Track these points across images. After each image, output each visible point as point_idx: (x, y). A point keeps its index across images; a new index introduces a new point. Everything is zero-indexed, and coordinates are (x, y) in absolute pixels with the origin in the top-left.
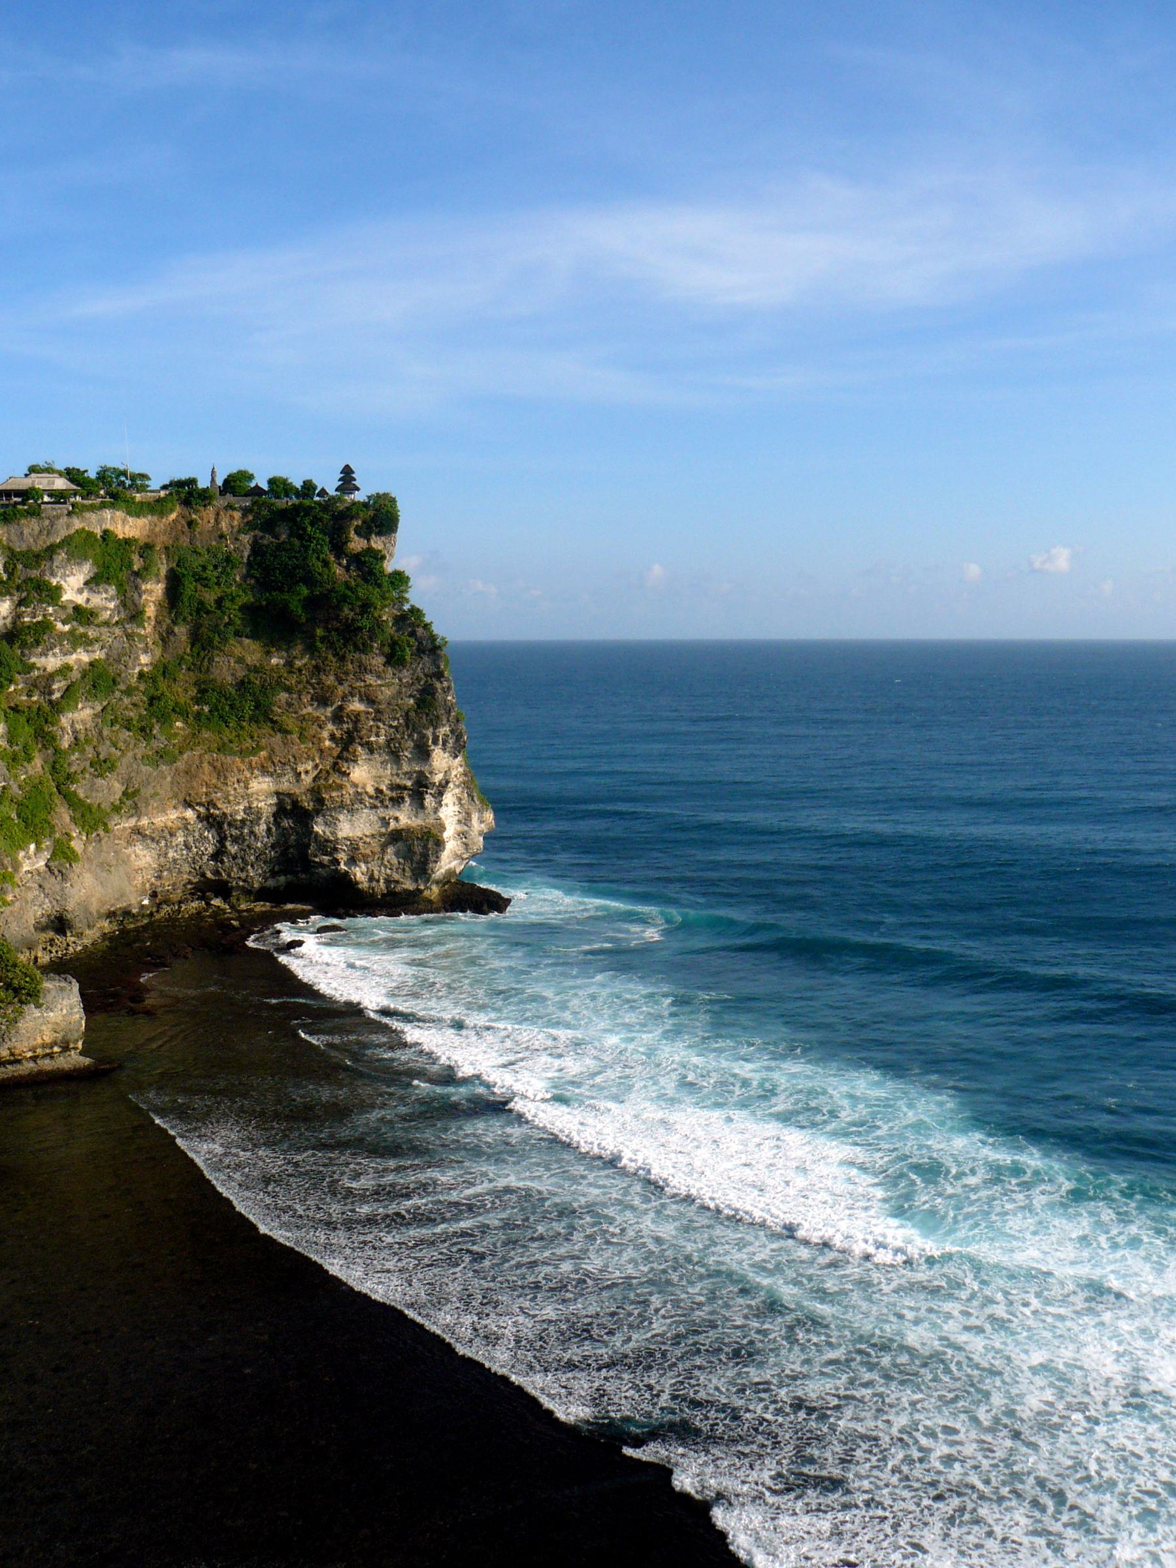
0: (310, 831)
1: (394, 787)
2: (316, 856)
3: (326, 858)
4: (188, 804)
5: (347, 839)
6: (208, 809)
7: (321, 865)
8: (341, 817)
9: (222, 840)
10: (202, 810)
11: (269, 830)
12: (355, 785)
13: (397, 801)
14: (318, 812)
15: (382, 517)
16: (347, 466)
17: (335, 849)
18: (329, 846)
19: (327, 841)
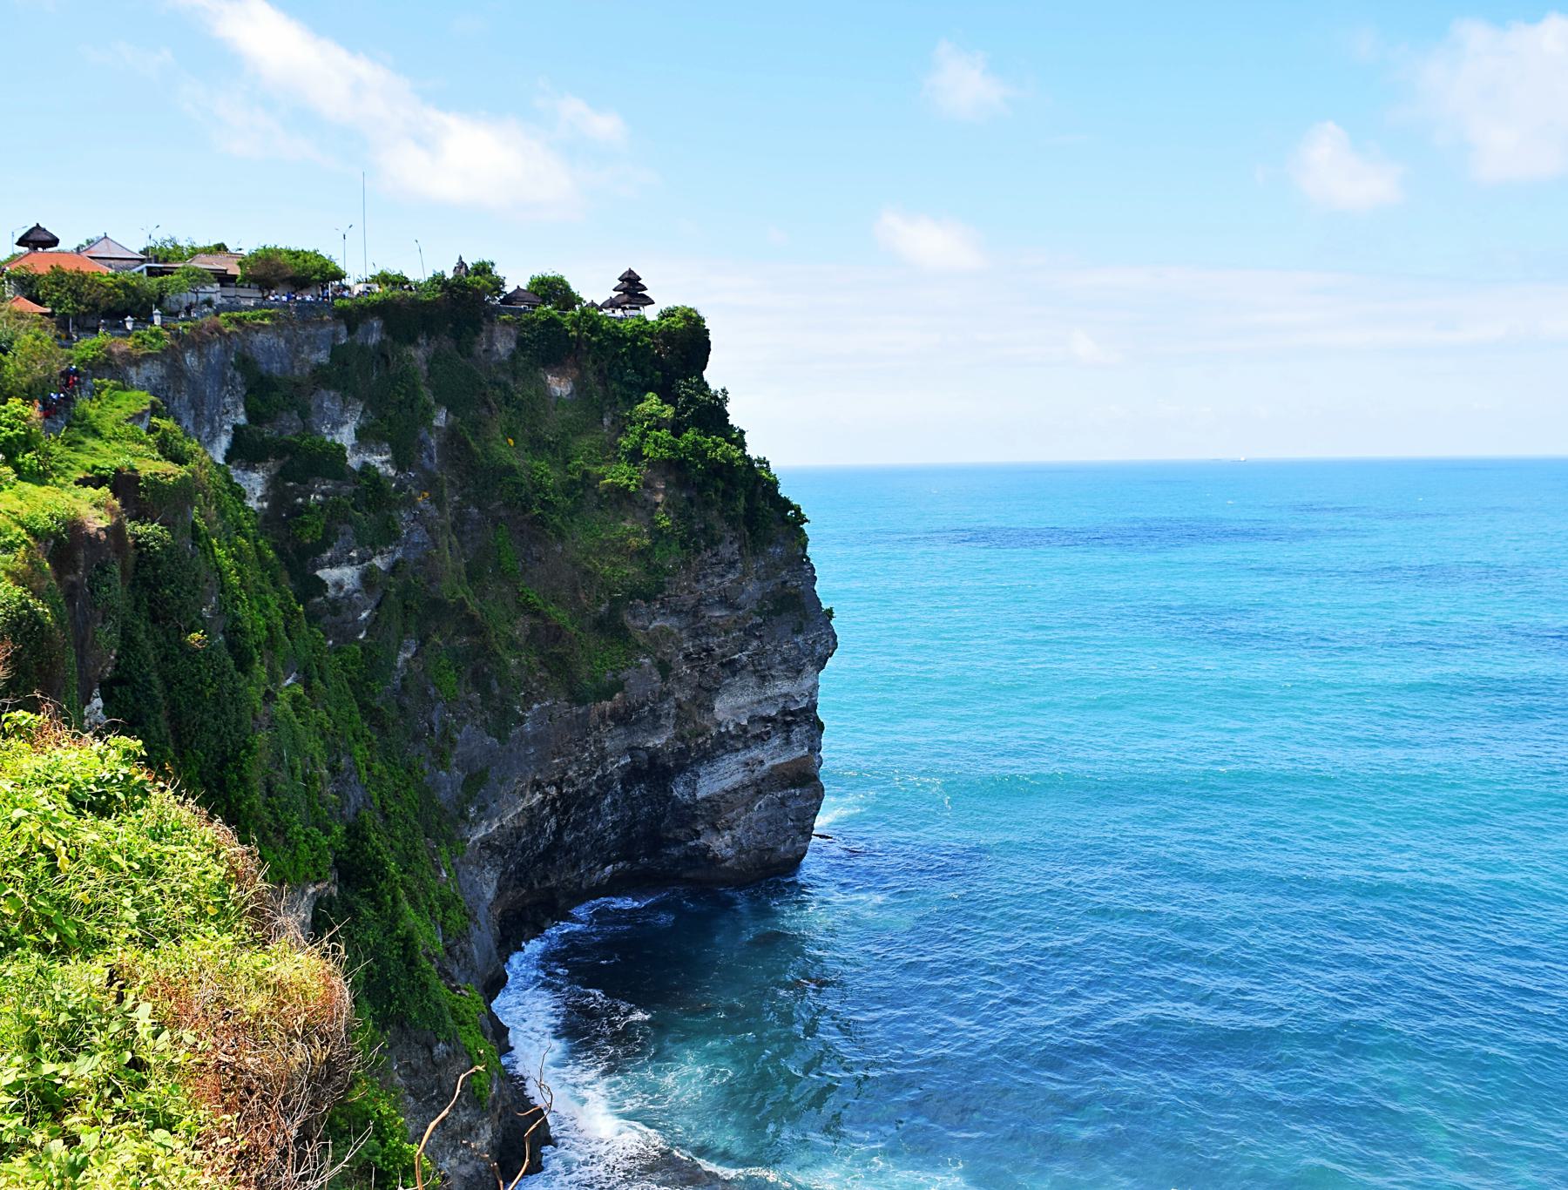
0: (668, 796)
1: (752, 720)
2: (669, 830)
3: (681, 833)
4: (537, 786)
5: (707, 799)
6: (559, 788)
7: (678, 842)
8: (702, 772)
9: (558, 833)
10: (553, 791)
11: (614, 803)
12: (719, 724)
13: (761, 739)
14: (681, 769)
15: (688, 341)
16: (630, 272)
17: (695, 817)
18: (687, 815)
19: (688, 807)
